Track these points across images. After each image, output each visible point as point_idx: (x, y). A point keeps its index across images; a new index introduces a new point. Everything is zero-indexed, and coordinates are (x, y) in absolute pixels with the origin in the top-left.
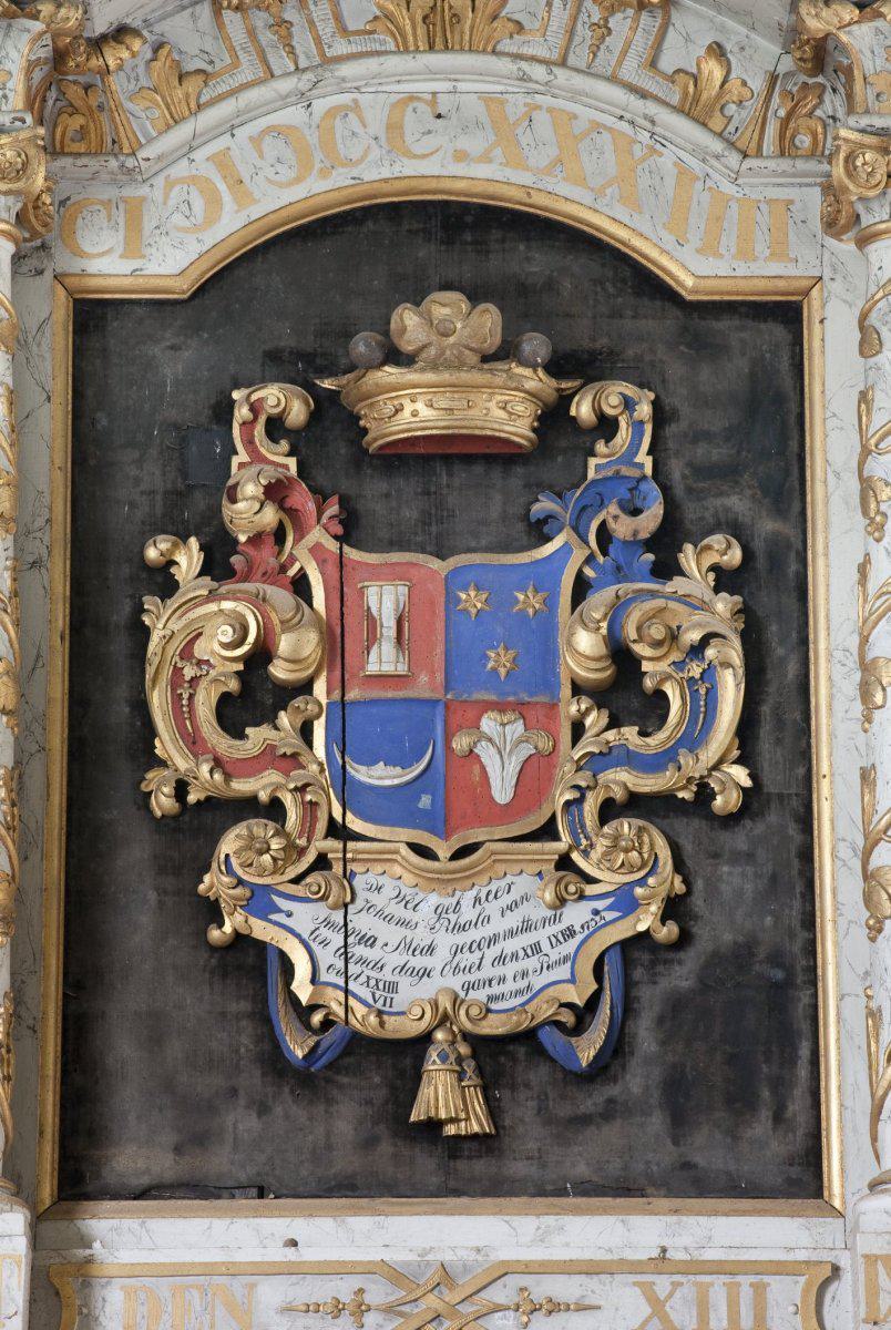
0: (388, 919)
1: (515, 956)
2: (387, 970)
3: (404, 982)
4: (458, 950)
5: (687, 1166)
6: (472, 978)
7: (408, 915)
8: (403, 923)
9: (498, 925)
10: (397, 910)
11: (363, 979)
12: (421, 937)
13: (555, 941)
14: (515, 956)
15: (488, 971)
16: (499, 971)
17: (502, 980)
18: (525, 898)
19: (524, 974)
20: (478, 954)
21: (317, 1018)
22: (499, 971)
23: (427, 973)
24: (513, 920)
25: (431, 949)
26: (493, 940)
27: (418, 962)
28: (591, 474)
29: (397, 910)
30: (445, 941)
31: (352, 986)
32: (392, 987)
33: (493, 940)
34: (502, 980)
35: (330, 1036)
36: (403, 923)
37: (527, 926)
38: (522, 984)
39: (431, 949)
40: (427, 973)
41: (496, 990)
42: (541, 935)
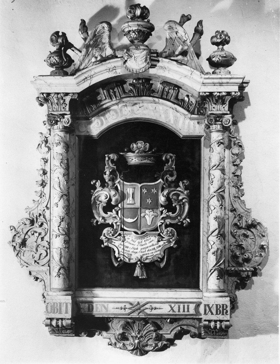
0: (130, 244)
1: (151, 250)
2: (130, 252)
3: (133, 254)
4: (142, 249)
5: (178, 283)
6: (144, 253)
7: (134, 243)
8: (132, 244)
9: (148, 245)
10: (132, 242)
11: (126, 253)
12: (136, 247)
13: (157, 247)
14: (151, 250)
15: (146, 252)
16: (148, 252)
17: (149, 254)
18: (153, 240)
19: (152, 253)
20: (145, 250)
21: (119, 260)
22: (148, 252)
23: (137, 253)
24: (151, 244)
25: (137, 249)
26: (147, 247)
27: (135, 251)
28: (165, 169)
29: (132, 242)
30: (140, 248)
31: (125, 254)
32: (131, 255)
33: (147, 247)
34: (149, 254)
35: (121, 263)
36: (132, 244)
37: (153, 245)
38: (152, 254)
39: (137, 249)
40: (137, 253)
41: (148, 255)
42: (155, 247)
